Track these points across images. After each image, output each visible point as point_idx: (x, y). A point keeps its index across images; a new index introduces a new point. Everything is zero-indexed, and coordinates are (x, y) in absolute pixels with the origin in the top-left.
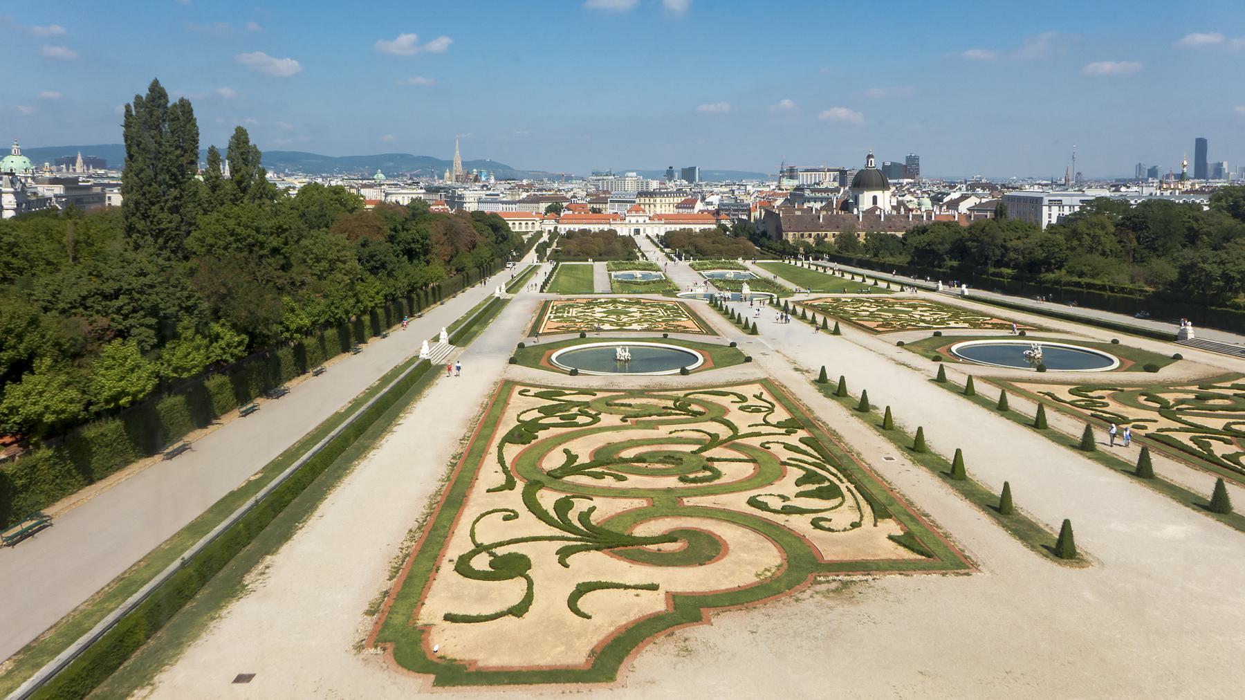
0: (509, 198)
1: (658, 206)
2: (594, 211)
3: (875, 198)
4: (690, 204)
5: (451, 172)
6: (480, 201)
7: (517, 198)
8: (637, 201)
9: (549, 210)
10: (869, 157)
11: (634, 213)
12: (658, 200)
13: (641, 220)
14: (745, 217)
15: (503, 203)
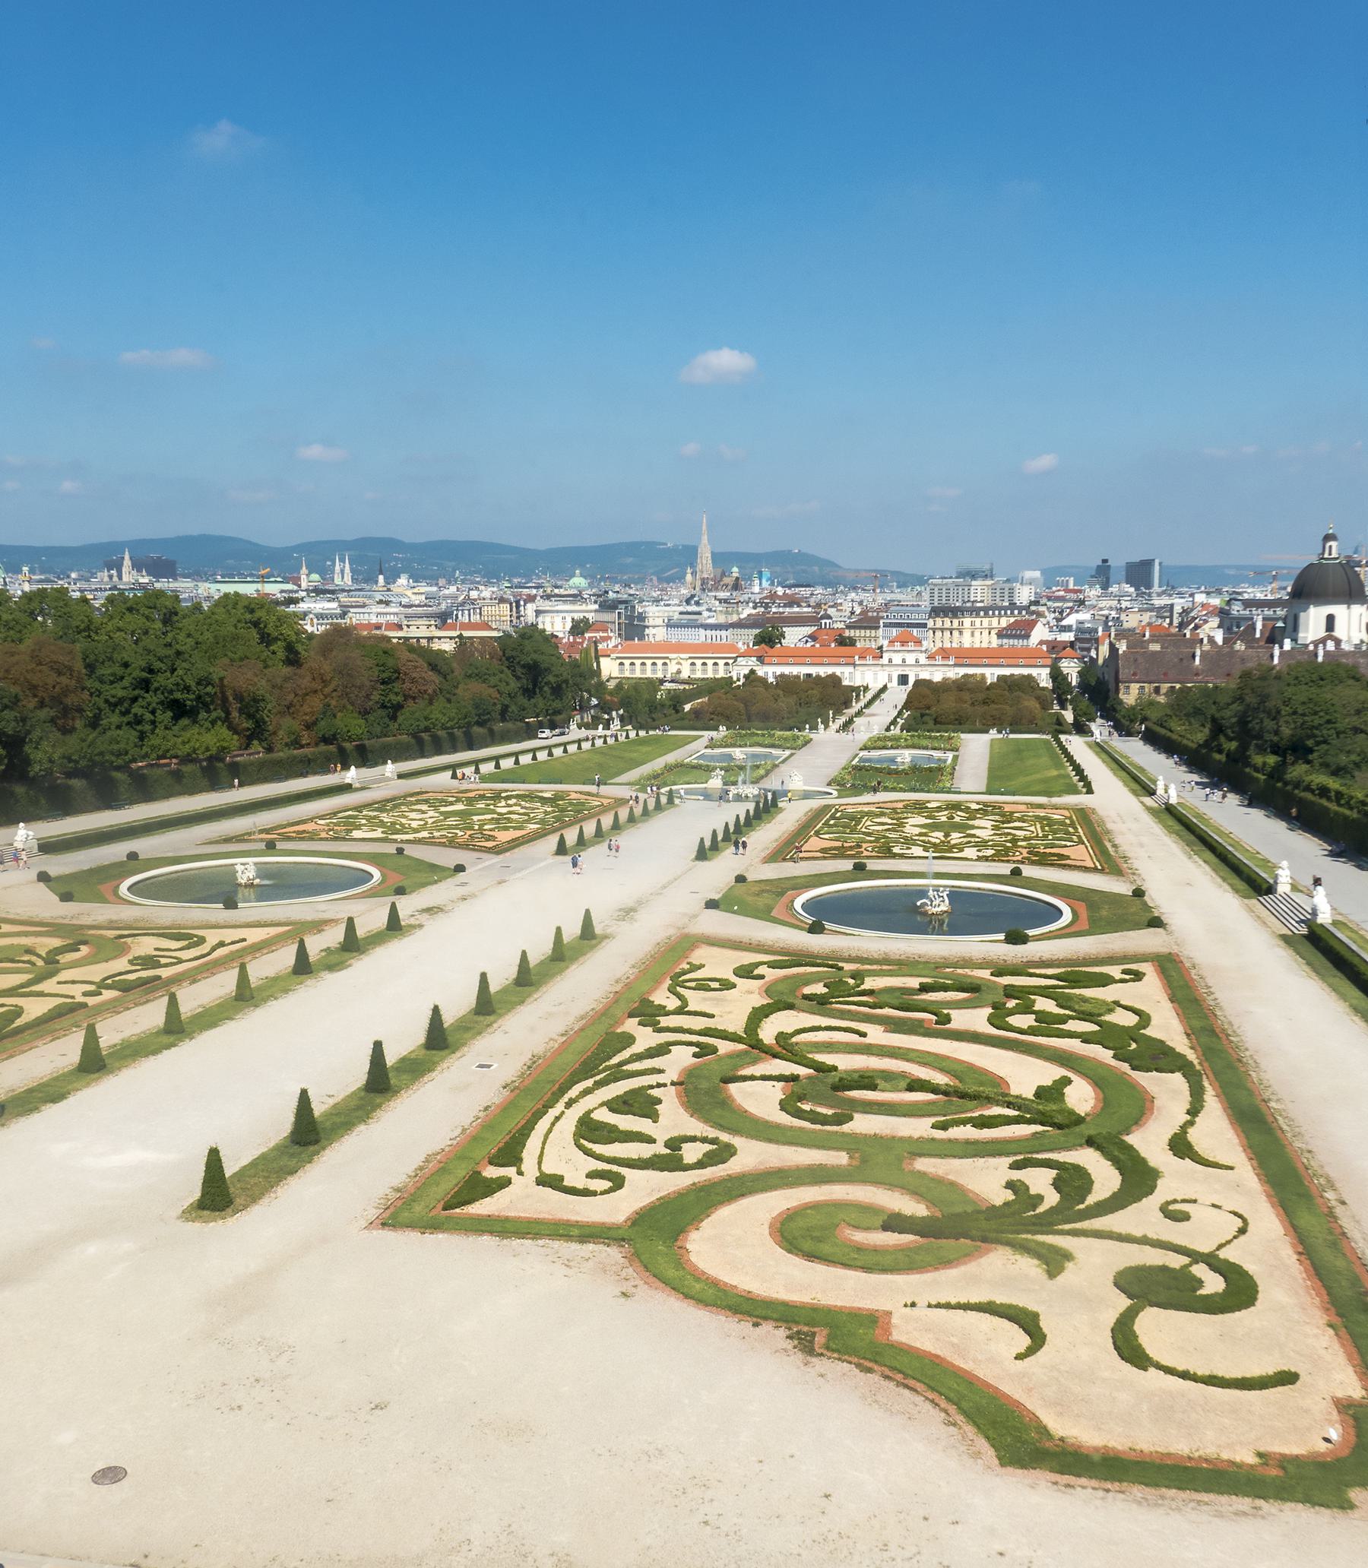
0: (722, 619)
1: (967, 634)
2: (843, 642)
3: (1330, 620)
4: (1021, 630)
5: (694, 573)
6: (670, 625)
7: (735, 618)
8: (930, 623)
9: (760, 640)
10: (1328, 538)
11: (898, 646)
12: (967, 621)
13: (910, 659)
14: (1093, 654)
15: (706, 627)
